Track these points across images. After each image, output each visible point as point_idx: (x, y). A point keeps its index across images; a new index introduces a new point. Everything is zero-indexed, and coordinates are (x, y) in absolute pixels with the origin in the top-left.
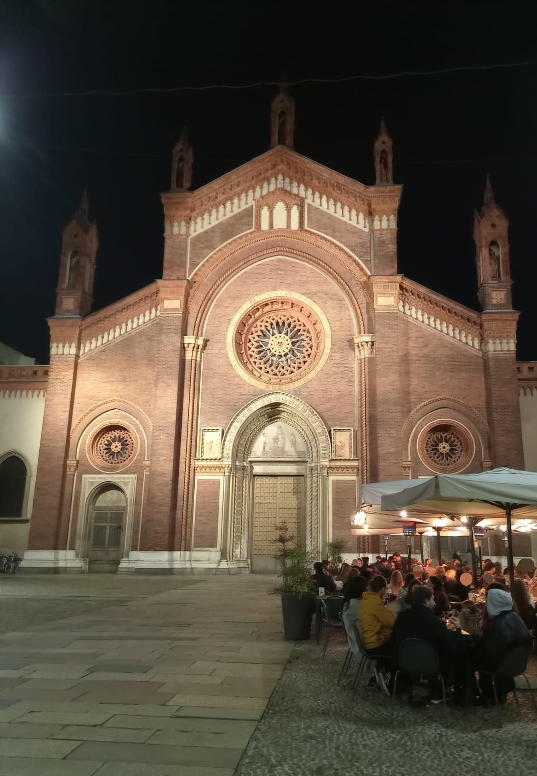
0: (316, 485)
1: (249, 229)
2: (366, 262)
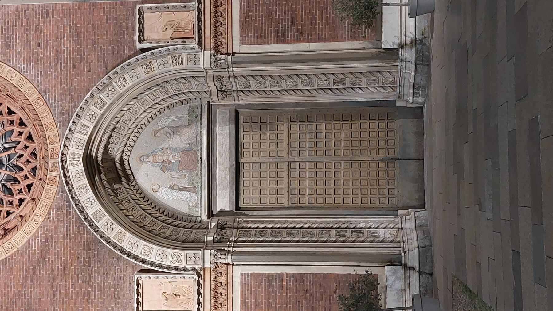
0: (252, 81)
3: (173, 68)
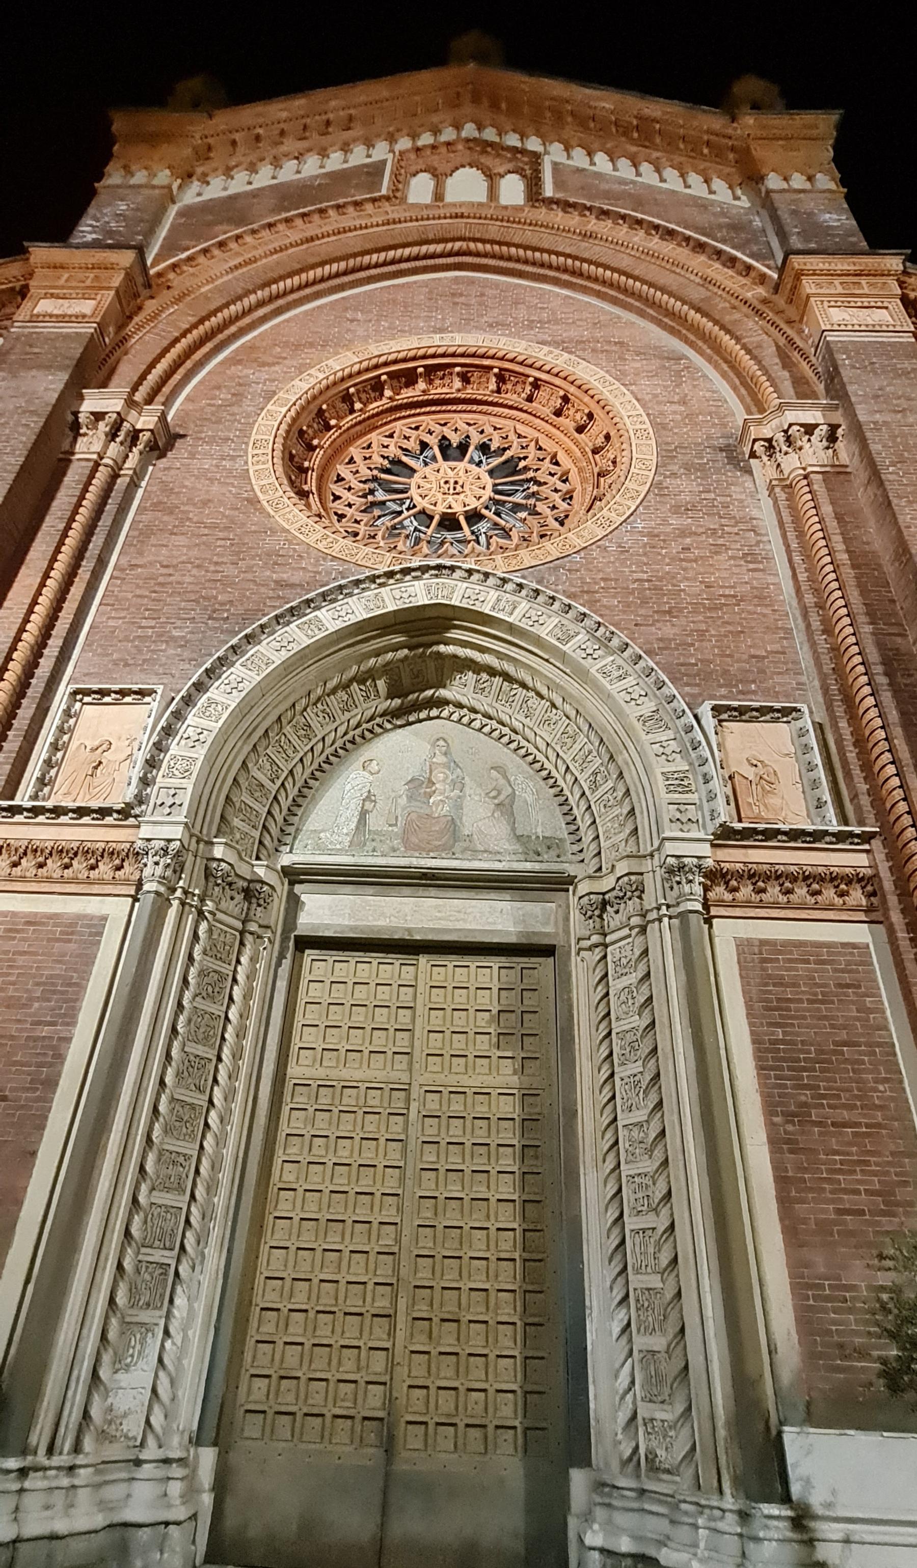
3: (658, 772)
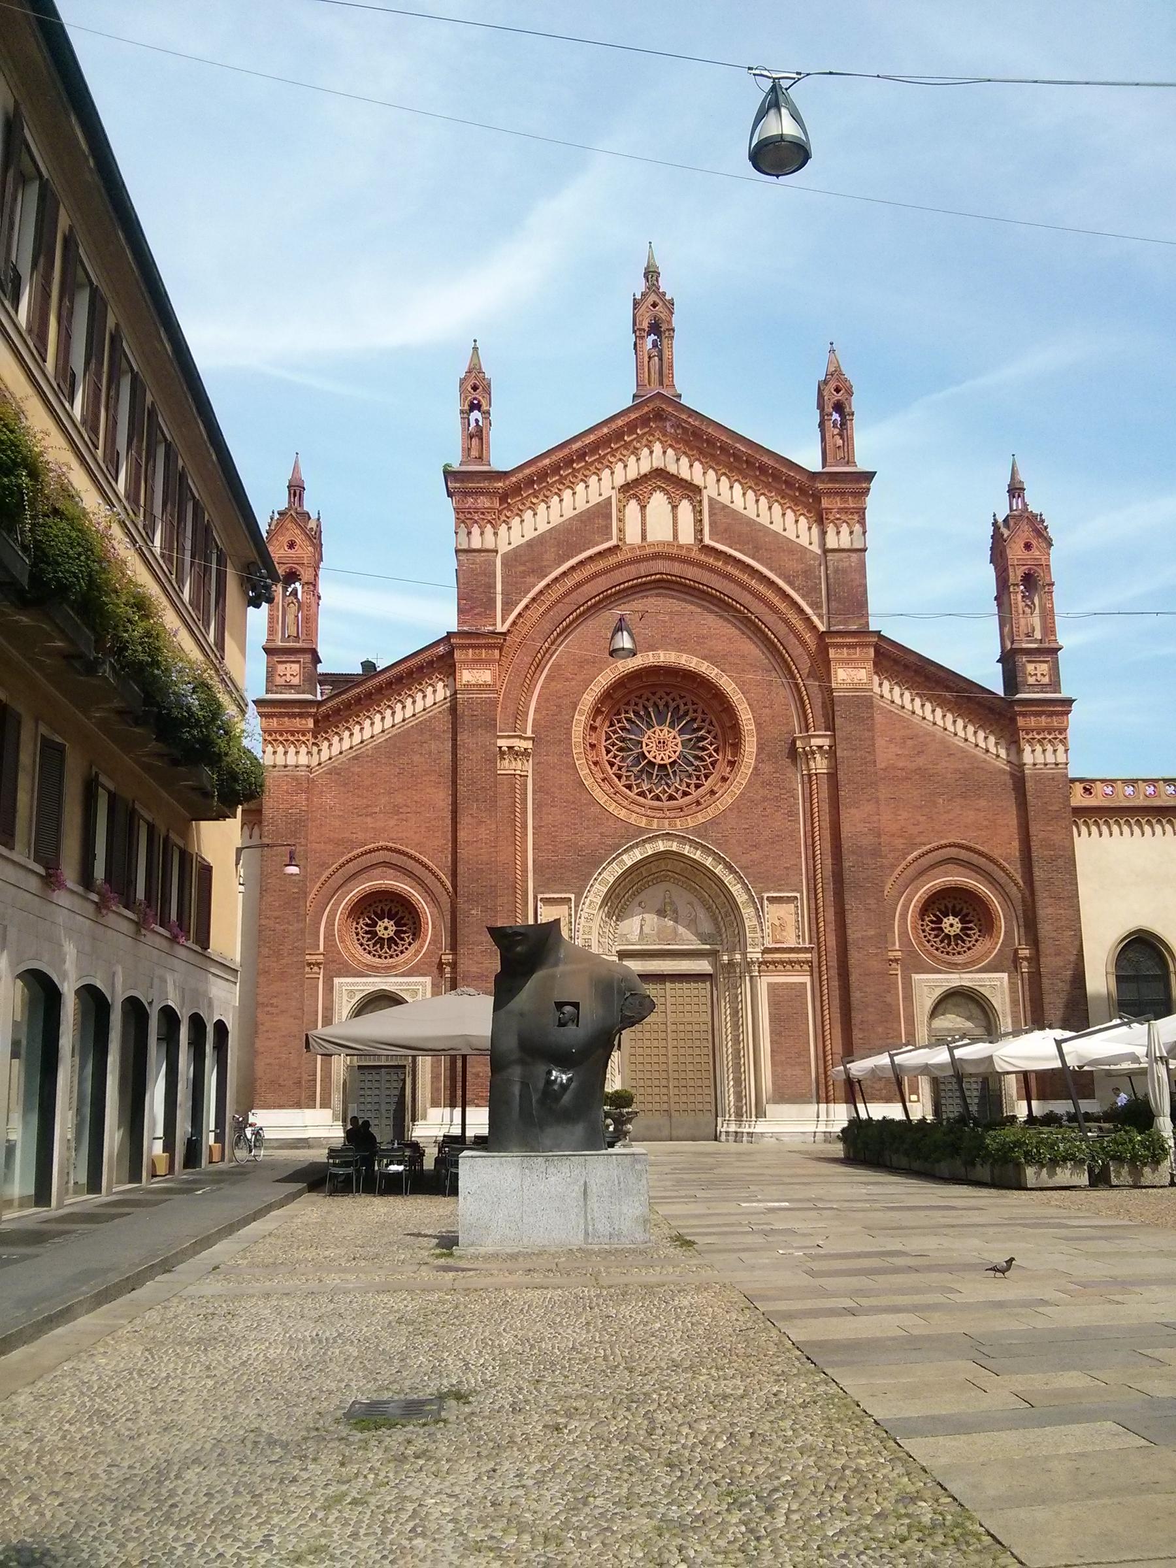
1: (608, 540)
2: (816, 606)
